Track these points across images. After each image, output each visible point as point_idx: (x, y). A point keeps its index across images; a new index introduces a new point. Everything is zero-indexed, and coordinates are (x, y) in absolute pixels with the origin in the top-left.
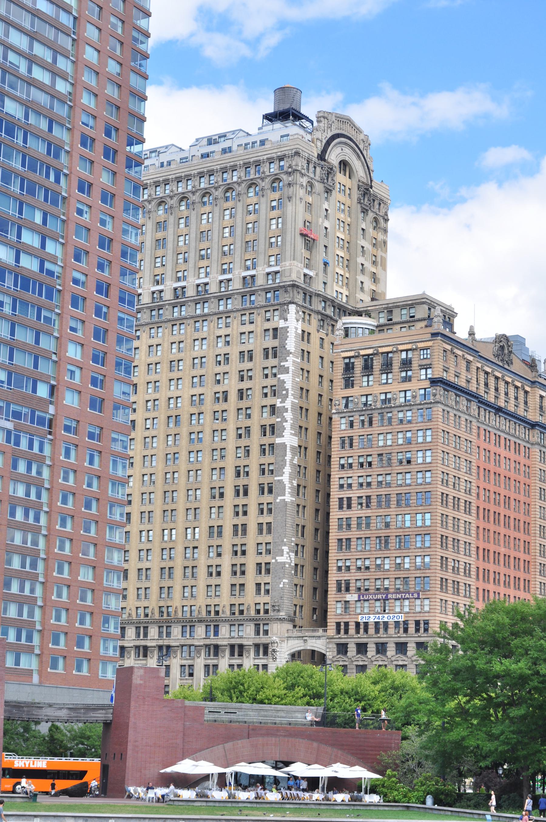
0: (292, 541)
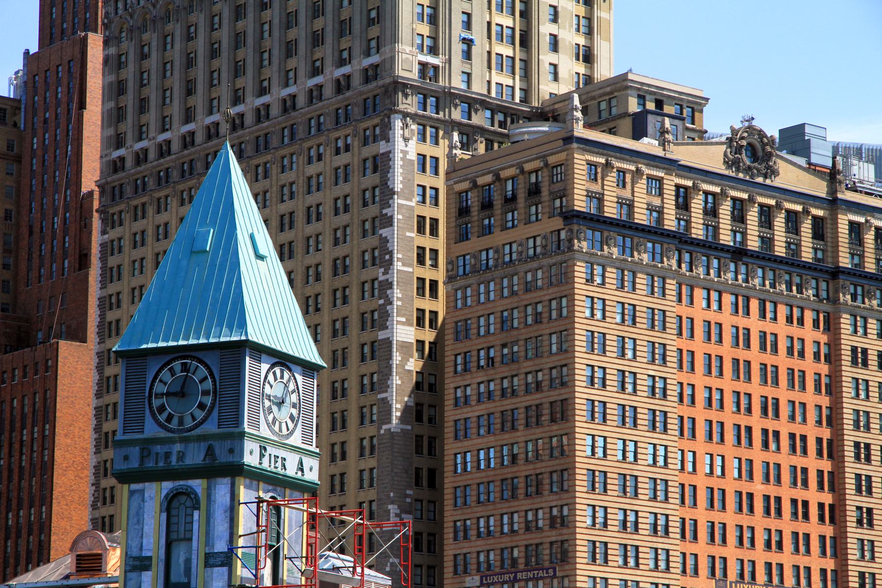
0: (407, 496)
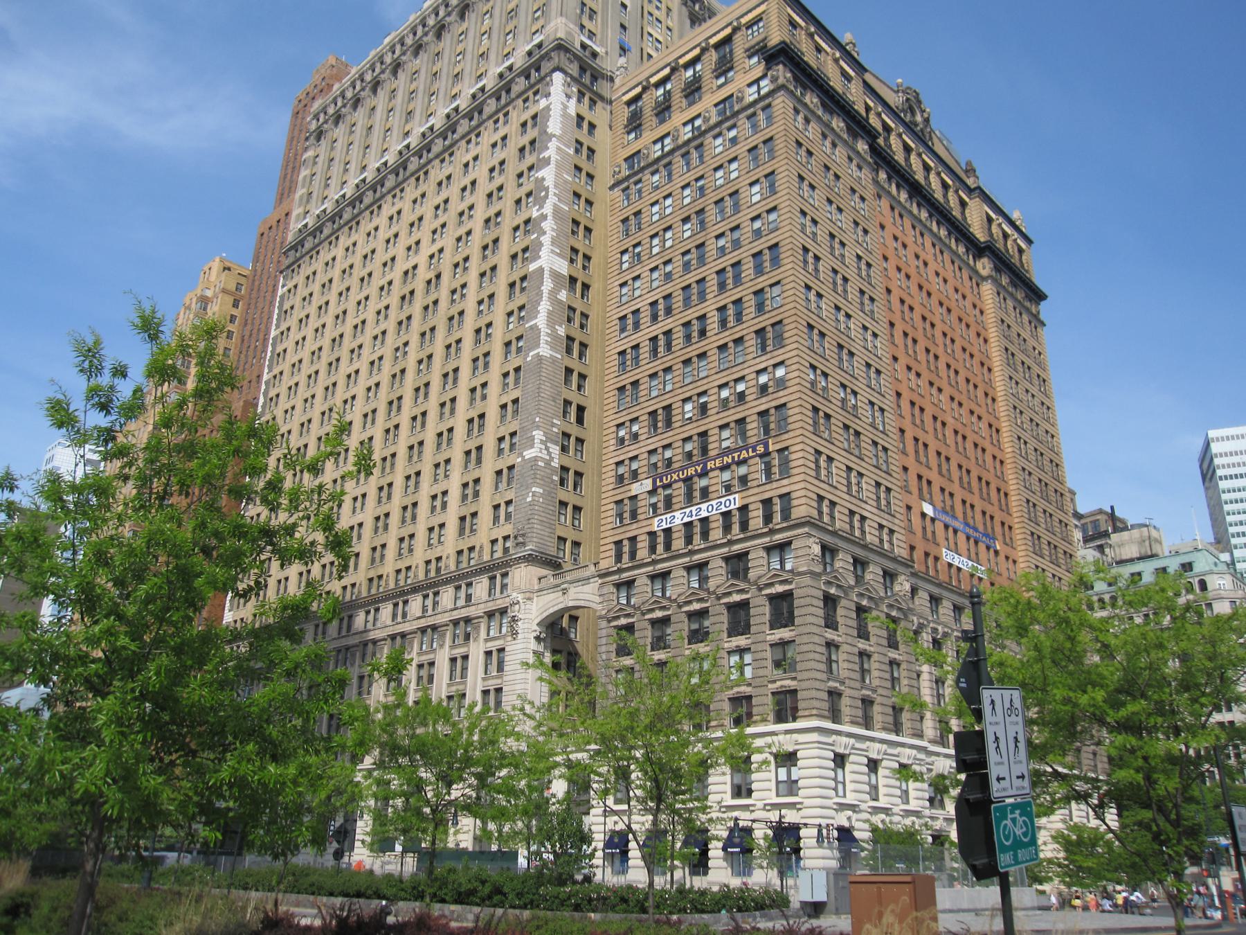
0: (553, 425)
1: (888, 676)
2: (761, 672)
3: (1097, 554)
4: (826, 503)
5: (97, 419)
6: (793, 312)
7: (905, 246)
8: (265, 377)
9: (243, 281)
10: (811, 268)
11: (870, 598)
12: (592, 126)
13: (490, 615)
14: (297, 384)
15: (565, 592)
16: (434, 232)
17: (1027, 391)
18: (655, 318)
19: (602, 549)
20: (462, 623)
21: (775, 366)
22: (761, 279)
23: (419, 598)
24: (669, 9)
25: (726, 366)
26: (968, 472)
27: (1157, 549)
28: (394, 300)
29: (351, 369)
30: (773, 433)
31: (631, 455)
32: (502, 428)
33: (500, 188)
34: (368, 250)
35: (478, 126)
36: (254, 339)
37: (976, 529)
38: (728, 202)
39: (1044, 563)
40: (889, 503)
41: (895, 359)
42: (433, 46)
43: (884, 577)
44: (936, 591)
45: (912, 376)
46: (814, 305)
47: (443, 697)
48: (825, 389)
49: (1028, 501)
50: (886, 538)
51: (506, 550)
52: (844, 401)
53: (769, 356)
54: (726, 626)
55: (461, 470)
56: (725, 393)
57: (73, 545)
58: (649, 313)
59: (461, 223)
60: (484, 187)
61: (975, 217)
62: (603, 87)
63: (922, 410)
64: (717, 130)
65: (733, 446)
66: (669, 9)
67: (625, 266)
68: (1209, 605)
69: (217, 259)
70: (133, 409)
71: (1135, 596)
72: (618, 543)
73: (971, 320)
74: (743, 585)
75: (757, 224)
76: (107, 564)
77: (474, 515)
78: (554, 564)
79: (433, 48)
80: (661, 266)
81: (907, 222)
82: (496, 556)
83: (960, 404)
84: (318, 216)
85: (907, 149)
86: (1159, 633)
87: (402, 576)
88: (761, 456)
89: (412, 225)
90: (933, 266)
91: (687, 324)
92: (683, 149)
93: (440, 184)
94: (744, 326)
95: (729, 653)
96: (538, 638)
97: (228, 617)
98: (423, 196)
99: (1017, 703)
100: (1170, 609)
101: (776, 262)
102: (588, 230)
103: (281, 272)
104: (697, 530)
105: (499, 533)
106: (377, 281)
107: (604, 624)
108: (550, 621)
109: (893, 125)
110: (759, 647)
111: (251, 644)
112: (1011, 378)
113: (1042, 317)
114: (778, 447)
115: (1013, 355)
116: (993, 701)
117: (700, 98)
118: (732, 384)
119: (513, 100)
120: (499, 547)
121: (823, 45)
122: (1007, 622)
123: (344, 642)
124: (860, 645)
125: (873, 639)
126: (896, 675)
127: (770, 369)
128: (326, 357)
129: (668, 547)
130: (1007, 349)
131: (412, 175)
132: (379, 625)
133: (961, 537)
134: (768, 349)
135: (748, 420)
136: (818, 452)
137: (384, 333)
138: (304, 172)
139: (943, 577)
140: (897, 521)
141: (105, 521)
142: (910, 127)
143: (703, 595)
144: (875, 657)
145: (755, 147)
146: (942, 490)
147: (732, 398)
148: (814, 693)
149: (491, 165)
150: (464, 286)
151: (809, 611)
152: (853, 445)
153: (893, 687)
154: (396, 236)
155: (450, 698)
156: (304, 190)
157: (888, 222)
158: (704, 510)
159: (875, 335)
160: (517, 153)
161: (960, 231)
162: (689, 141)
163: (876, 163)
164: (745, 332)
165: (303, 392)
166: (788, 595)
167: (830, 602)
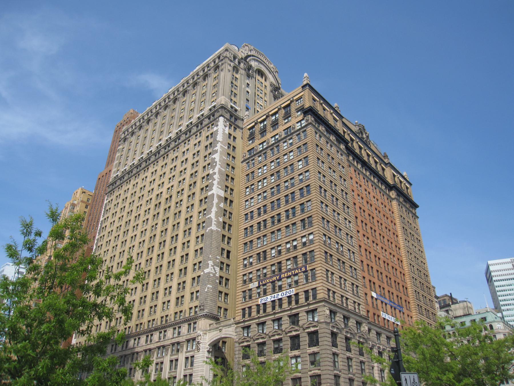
0: (217, 259)
1: (359, 368)
2: (305, 367)
3: (446, 314)
4: (331, 292)
5: (26, 254)
6: (316, 212)
7: (361, 186)
8: (97, 237)
9: (90, 197)
10: (323, 194)
11: (351, 333)
12: (235, 138)
13: (188, 341)
14: (110, 240)
15: (220, 330)
16: (170, 179)
17: (413, 245)
18: (259, 214)
19: (237, 312)
20: (176, 345)
21: (309, 234)
22: (303, 199)
23: (158, 333)
24: (265, 94)
25: (289, 234)
26: (390, 279)
27: (471, 312)
28: (152, 206)
29: (133, 235)
30: (308, 262)
31: (249, 271)
32: (196, 260)
33: (197, 162)
34: (142, 186)
35: (189, 137)
36: (94, 221)
37: (394, 303)
38: (289, 168)
39: (424, 318)
40: (357, 292)
41: (358, 232)
42: (172, 106)
43: (357, 324)
44: (379, 330)
45: (365, 239)
46: (324, 210)
47: (167, 378)
48: (330, 244)
49: (416, 291)
50: (357, 307)
51: (196, 312)
52: (337, 249)
53: (306, 230)
54: (289, 346)
55: (178, 277)
56: (288, 246)
57: (9, 308)
58: (257, 212)
59: (181, 175)
60: (191, 161)
61: (388, 174)
62: (239, 123)
63: (370, 253)
64: (285, 140)
65: (292, 268)
66: (265, 94)
67: (247, 193)
68: (495, 336)
69: (80, 189)
70: (42, 250)
71: (464, 332)
72: (244, 309)
73: (389, 216)
74: (297, 328)
75: (301, 177)
76: (24, 317)
77: (183, 297)
78: (216, 318)
79: (172, 107)
80: (262, 194)
81: (361, 176)
82: (192, 314)
83: (386, 250)
84: (123, 172)
85: (360, 148)
86: (475, 348)
87: (151, 323)
88: (304, 272)
89: (161, 176)
90: (372, 194)
91: (273, 217)
92: (271, 147)
93: (173, 160)
94: (296, 218)
95: (291, 358)
96: (208, 351)
97: (74, 341)
98: (166, 164)
99: (417, 380)
100: (479, 338)
101: (309, 192)
102: (232, 179)
103: (106, 194)
104: (277, 304)
105: (193, 305)
106: (146, 198)
107: (237, 345)
108: (215, 343)
109: (354, 139)
110: (304, 355)
111: (83, 354)
112: (406, 239)
113: (417, 214)
114: (311, 268)
115: (406, 230)
116: (406, 379)
117: (278, 128)
118: (291, 242)
119: (203, 128)
120: (193, 311)
121: (326, 108)
122: (409, 343)
123: (124, 353)
124: (347, 354)
125: (353, 352)
126: (363, 367)
127: (307, 236)
128: (123, 229)
129: (265, 311)
130: (404, 228)
131: (162, 156)
132: (140, 345)
133: (388, 307)
134: (306, 227)
135: (298, 257)
136: (327, 271)
137: (147, 219)
138: (118, 154)
139: (381, 324)
140: (361, 300)
141: (25, 298)
142: (361, 139)
143: (280, 332)
144: (354, 360)
145: (300, 147)
146: (380, 286)
147: (291, 248)
148: (328, 376)
149: (194, 153)
150: (181, 201)
151: (325, 339)
152: (342, 268)
153: (362, 373)
154: (154, 180)
155: (169, 378)
156: (118, 161)
157: (354, 176)
158: (280, 295)
159: (350, 222)
160: (204, 148)
161: (382, 180)
162: (273, 144)
163: (348, 153)
164: (296, 221)
165: (112, 244)
166: (316, 332)
167: (334, 335)
